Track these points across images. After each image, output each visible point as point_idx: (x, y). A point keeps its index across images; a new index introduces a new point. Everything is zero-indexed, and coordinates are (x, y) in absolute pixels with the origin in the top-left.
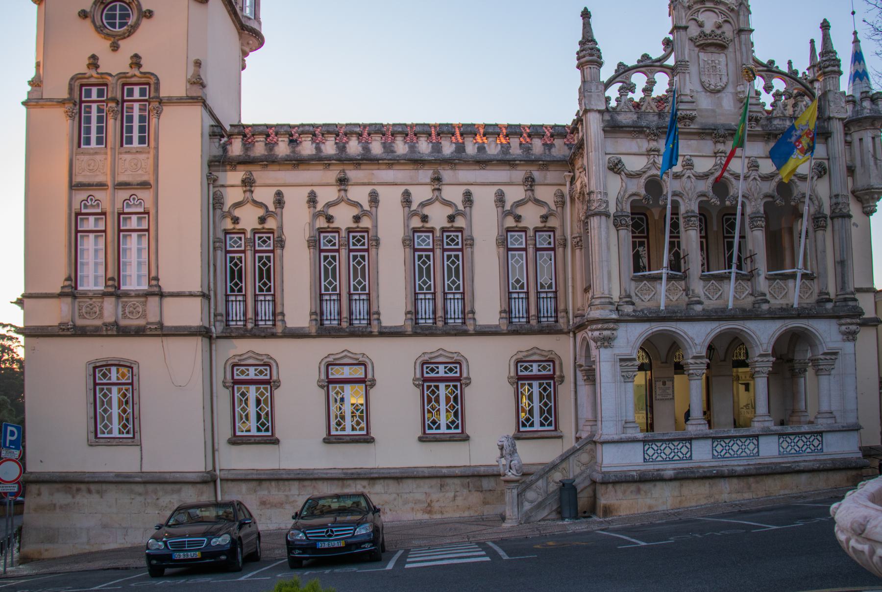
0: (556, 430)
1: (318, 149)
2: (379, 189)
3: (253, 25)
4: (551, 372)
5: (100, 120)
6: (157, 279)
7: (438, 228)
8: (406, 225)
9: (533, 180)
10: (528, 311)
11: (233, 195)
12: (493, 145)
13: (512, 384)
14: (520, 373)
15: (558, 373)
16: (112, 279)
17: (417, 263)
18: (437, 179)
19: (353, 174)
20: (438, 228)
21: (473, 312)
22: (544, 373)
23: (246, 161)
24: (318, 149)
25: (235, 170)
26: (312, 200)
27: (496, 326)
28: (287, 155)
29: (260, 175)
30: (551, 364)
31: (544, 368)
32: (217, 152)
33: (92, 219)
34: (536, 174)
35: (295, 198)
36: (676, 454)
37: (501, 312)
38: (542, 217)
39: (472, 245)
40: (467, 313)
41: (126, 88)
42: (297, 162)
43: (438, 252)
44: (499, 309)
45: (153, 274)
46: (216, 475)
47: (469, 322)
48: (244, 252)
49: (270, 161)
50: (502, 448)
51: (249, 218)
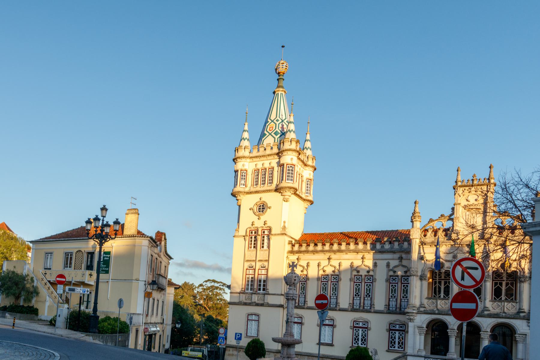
4: (404, 329)
7: (363, 274)
8: (351, 274)
13: (388, 332)
14: (391, 328)
15: (406, 330)
17: (355, 287)
20: (363, 274)
21: (374, 305)
22: (401, 329)
27: (382, 310)
31: (401, 327)
37: (385, 306)
39: (375, 281)
40: (372, 305)
41: (263, 231)
43: (363, 283)
44: (384, 304)
47: (372, 308)
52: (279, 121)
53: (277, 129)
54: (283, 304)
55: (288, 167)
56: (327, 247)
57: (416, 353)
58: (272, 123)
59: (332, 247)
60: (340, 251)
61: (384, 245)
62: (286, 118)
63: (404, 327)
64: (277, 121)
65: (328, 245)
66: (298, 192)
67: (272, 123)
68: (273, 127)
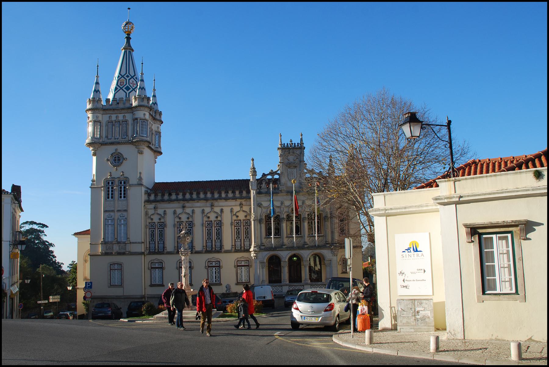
0: (249, 282)
1: (177, 197)
2: (195, 209)
3: (159, 150)
4: (248, 264)
5: (112, 191)
6: (129, 238)
9: (242, 204)
10: (241, 245)
11: (151, 212)
12: (230, 194)
14: (238, 265)
15: (250, 265)
16: (116, 239)
18: (212, 206)
19: (187, 204)
23: (155, 201)
24: (177, 197)
25: (152, 204)
26: (175, 212)
28: (168, 199)
29: (159, 205)
30: (248, 262)
32: (147, 199)
33: (110, 221)
34: (244, 203)
35: (170, 212)
36: (277, 290)
38: (245, 216)
40: (221, 246)
42: (170, 201)
43: (213, 228)
45: (128, 237)
46: (145, 296)
48: (155, 229)
49: (163, 201)
50: (226, 287)
51: (156, 219)
52: (129, 76)
53: (128, 85)
54: (144, 251)
55: (142, 122)
56: (180, 197)
57: (261, 283)
58: (123, 78)
59: (185, 196)
60: (192, 199)
61: (228, 194)
62: (135, 75)
63: (248, 263)
64: (128, 76)
65: (181, 194)
66: (150, 145)
67: (123, 78)
68: (123, 82)
